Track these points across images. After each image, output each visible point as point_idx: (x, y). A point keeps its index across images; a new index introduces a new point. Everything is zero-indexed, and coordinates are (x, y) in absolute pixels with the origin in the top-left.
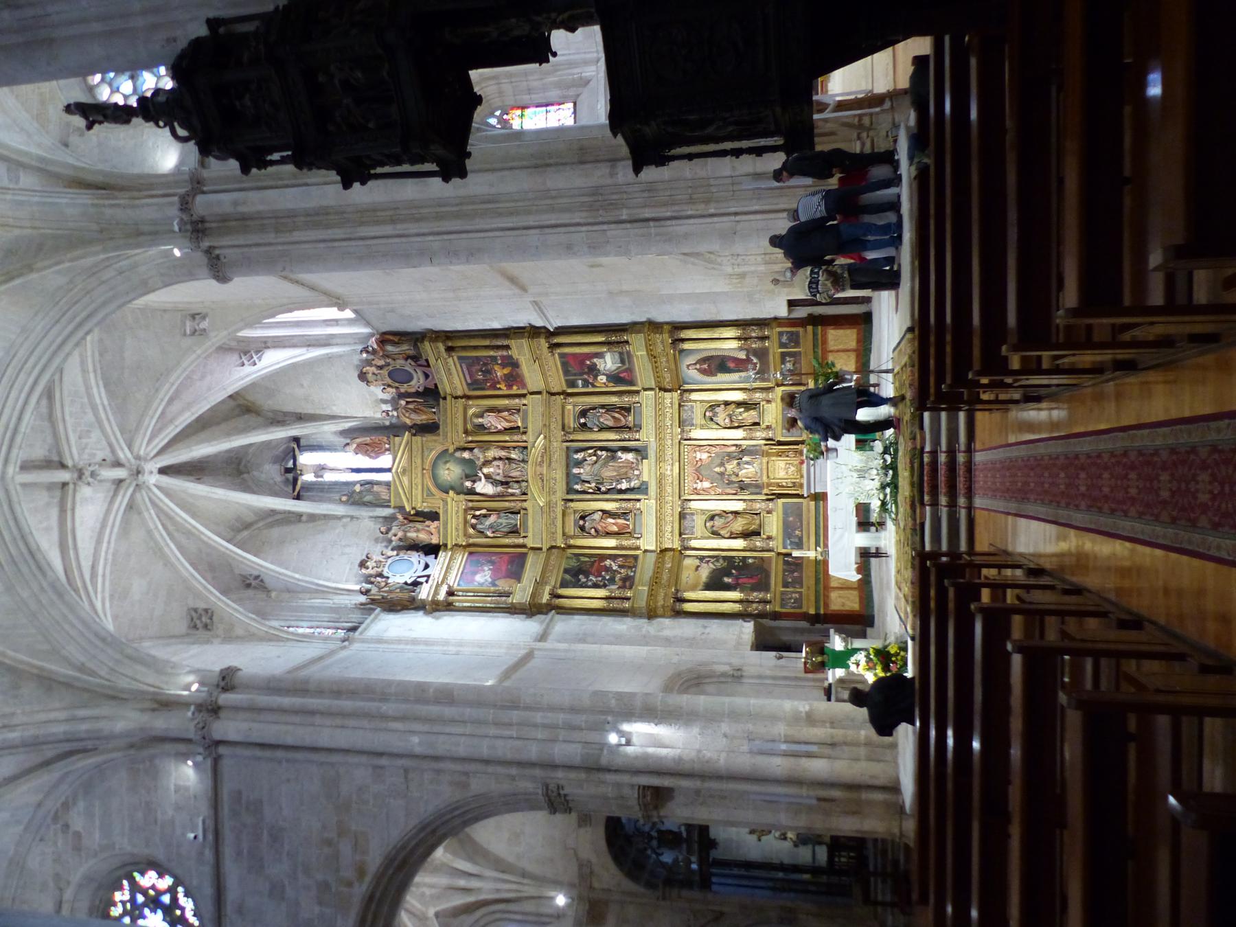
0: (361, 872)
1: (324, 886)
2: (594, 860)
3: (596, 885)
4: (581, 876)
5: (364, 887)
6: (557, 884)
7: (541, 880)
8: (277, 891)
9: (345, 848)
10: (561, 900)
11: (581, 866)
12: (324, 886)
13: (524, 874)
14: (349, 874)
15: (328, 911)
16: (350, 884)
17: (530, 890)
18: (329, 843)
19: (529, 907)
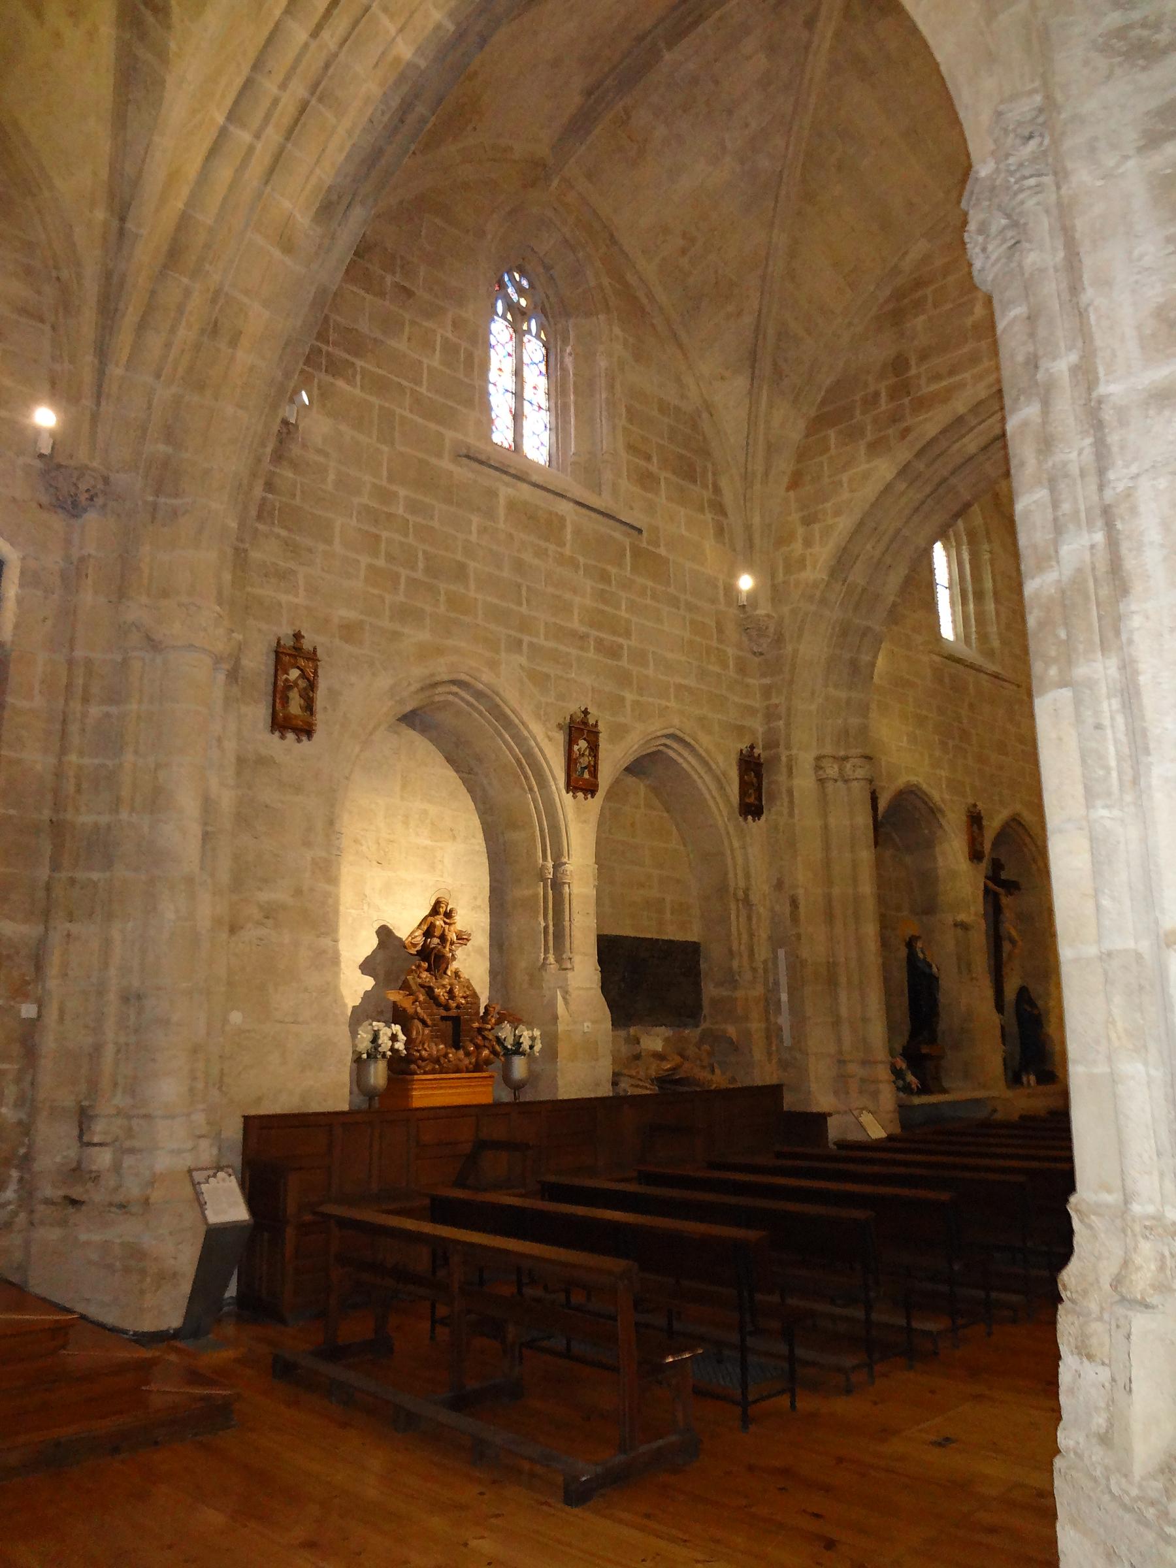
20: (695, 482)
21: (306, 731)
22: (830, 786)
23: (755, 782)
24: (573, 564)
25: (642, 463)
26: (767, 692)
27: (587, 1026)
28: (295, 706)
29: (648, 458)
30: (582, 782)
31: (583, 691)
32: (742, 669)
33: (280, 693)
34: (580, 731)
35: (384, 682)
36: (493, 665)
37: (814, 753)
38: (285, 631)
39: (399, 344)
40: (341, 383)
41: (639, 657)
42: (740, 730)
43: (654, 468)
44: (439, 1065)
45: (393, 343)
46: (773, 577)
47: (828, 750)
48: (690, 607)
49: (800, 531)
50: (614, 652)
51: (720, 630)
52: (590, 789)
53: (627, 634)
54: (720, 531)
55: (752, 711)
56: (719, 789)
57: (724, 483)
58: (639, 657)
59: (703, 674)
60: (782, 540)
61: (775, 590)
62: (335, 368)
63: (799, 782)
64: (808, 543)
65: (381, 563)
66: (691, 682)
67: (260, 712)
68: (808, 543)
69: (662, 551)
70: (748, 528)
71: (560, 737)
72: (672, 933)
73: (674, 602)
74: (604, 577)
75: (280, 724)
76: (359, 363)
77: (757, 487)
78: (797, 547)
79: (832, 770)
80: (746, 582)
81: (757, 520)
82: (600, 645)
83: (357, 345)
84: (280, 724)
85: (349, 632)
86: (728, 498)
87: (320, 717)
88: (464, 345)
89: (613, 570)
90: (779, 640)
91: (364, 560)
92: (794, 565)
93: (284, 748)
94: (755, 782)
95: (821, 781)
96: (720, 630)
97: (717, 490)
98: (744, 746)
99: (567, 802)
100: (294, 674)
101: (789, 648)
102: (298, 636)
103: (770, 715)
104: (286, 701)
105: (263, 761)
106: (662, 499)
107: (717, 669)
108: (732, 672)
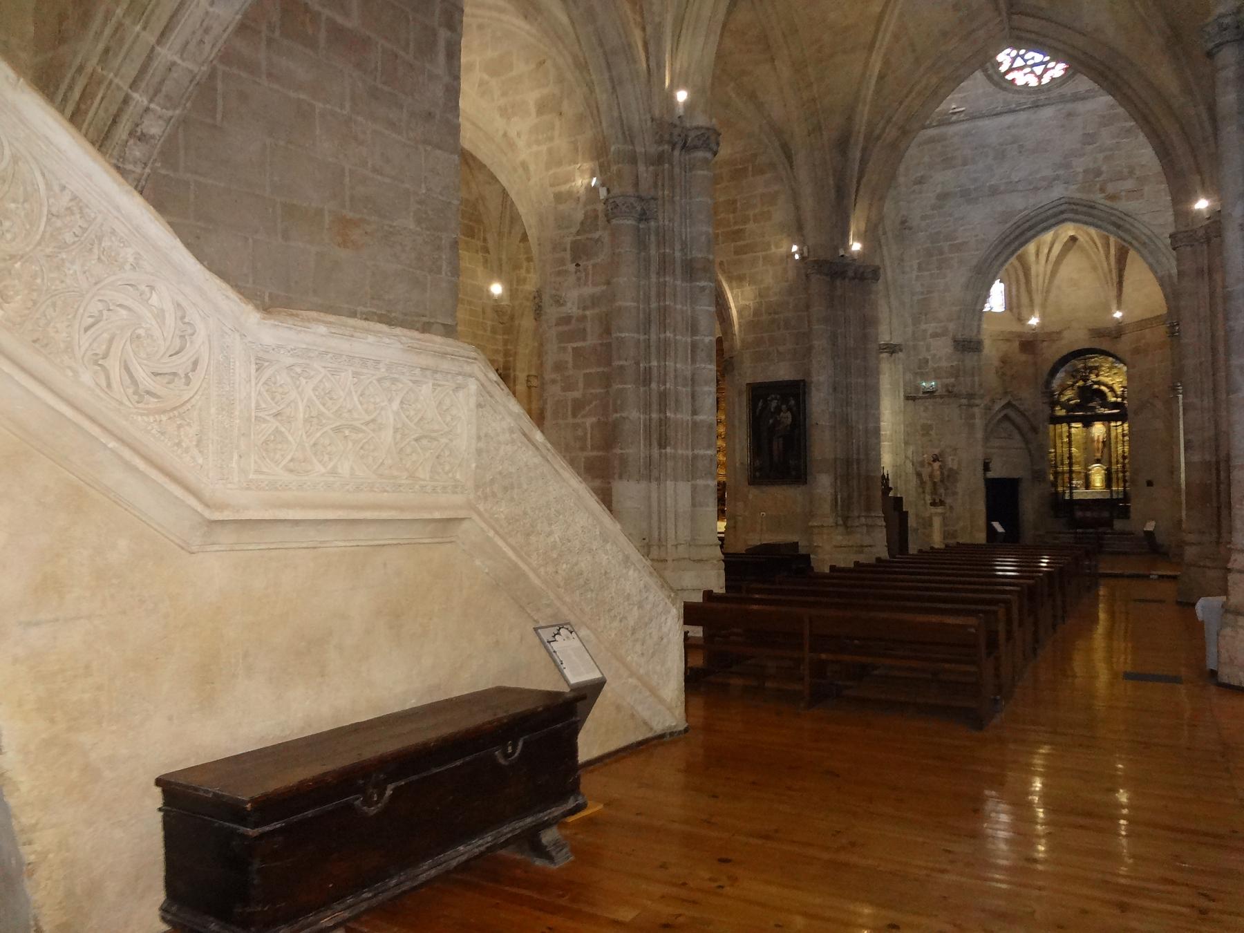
0: (1112, 198)
1: (1098, 173)
2: (1063, 342)
3: (1045, 344)
4: (1050, 334)
5: (1102, 201)
6: (1043, 317)
7: (1044, 306)
8: (1089, 138)
9: (1129, 184)
10: (1034, 321)
11: (1059, 333)
12: (1098, 173)
13: (1048, 291)
14: (1110, 188)
15: (1080, 177)
16: (1102, 190)
17: (1038, 299)
18: (1131, 172)
19: (1025, 299)
20: (473, 237)
22: (533, 390)
26: (506, 342)
32: (494, 331)
37: (526, 374)
46: (511, 285)
47: (533, 373)
48: (470, 303)
49: (525, 264)
51: (484, 312)
54: (486, 261)
55: (497, 351)
57: (488, 236)
60: (517, 267)
61: (512, 291)
64: (528, 271)
68: (528, 271)
70: (500, 260)
77: (505, 240)
78: (523, 272)
79: (534, 382)
81: (504, 257)
90: (512, 318)
92: (521, 281)
95: (529, 387)
96: (484, 312)
97: (485, 240)
101: (516, 323)
103: (506, 354)
107: (480, 332)
108: (489, 333)
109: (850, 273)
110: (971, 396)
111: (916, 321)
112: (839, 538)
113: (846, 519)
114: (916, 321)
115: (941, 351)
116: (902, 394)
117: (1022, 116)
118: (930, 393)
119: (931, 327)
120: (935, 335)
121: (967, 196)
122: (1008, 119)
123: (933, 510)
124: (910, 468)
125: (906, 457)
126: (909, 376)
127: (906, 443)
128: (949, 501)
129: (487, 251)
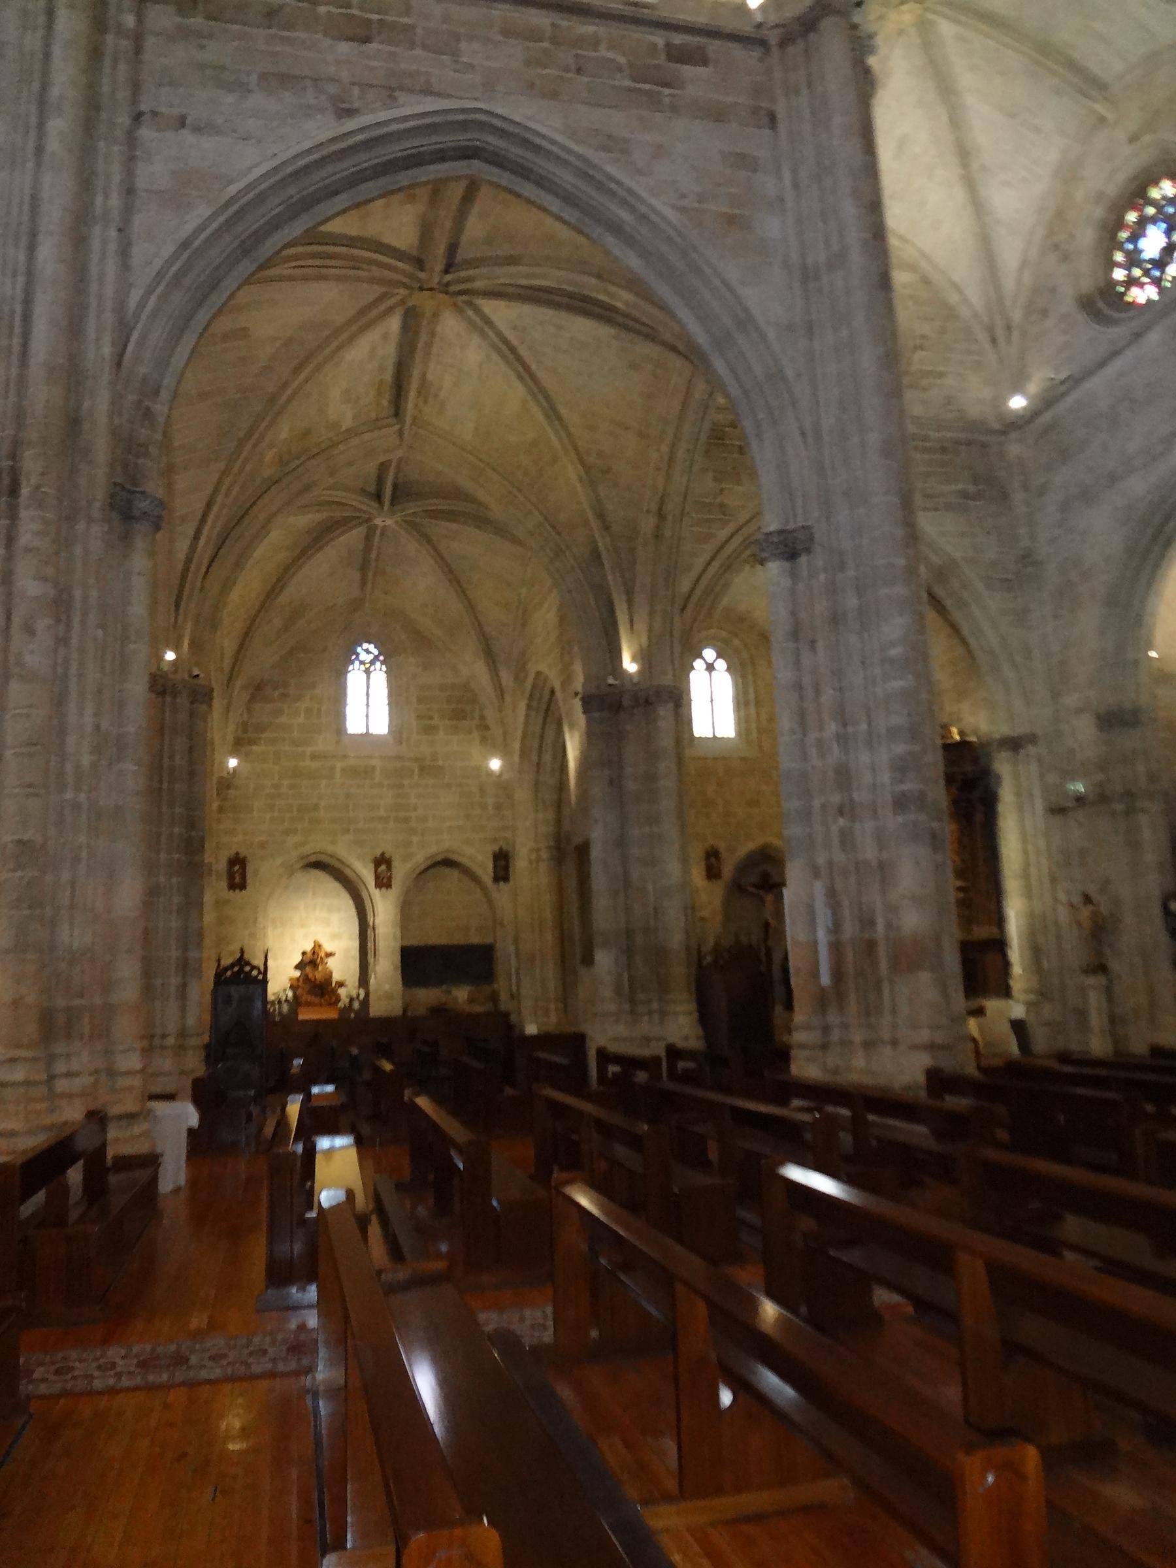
21: (242, 886)
23: (502, 864)
24: (381, 785)
25: (428, 722)
27: (387, 987)
28: (237, 880)
29: (431, 718)
30: (383, 883)
31: (385, 843)
33: (231, 877)
34: (382, 862)
35: (279, 861)
36: (332, 843)
38: (233, 852)
39: (283, 719)
40: (255, 748)
41: (425, 819)
42: (495, 840)
43: (436, 721)
44: (309, 1004)
45: (277, 721)
50: (407, 820)
52: (388, 886)
53: (415, 809)
56: (486, 871)
58: (425, 819)
59: (468, 816)
62: (252, 742)
63: (521, 864)
65: (276, 814)
66: (461, 823)
67: (224, 884)
69: (440, 763)
71: (372, 866)
72: (475, 939)
73: (449, 786)
74: (401, 786)
75: (232, 886)
76: (263, 736)
80: (495, 764)
82: (397, 820)
83: (262, 728)
84: (232, 886)
85: (263, 845)
86: (490, 721)
87: (249, 880)
88: (316, 706)
89: (406, 782)
91: (268, 816)
93: (237, 895)
94: (502, 864)
96: (482, 790)
97: (482, 718)
98: (497, 848)
99: (376, 894)
100: (237, 867)
102: (237, 854)
104: (234, 878)
105: (227, 902)
106: (441, 735)
109: (627, 702)
110: (1129, 795)
111: (1055, 695)
112: (621, 1030)
113: (632, 1001)
114: (1055, 695)
115: (1083, 733)
116: (1039, 806)
117: (1129, 354)
118: (1080, 799)
119: (1071, 700)
120: (1079, 711)
121: (1087, 496)
122: (1117, 365)
123: (1091, 980)
124: (1063, 914)
125: (1056, 899)
126: (1052, 778)
127: (1054, 880)
128: (1114, 965)
129: (487, 728)
